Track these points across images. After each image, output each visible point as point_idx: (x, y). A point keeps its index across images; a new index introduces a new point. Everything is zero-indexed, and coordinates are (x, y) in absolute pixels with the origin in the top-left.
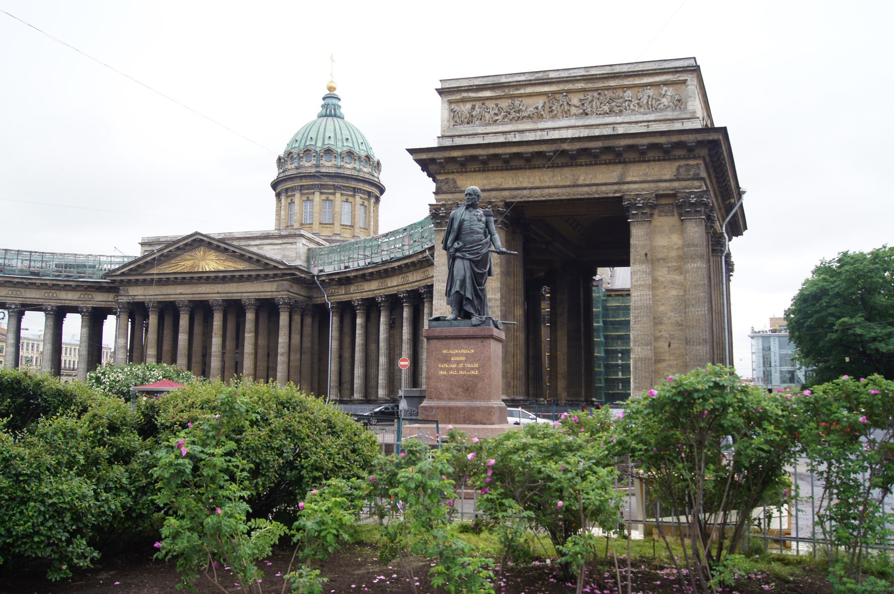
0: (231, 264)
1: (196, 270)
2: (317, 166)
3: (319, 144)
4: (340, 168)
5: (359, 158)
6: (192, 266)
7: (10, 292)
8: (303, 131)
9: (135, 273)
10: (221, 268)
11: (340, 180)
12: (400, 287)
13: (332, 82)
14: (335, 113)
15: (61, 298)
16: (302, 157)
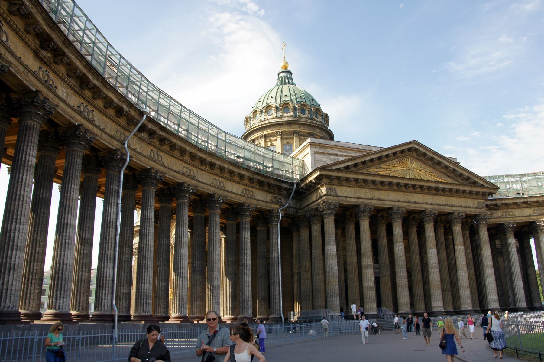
3: (308, 103)
15: (227, 189)
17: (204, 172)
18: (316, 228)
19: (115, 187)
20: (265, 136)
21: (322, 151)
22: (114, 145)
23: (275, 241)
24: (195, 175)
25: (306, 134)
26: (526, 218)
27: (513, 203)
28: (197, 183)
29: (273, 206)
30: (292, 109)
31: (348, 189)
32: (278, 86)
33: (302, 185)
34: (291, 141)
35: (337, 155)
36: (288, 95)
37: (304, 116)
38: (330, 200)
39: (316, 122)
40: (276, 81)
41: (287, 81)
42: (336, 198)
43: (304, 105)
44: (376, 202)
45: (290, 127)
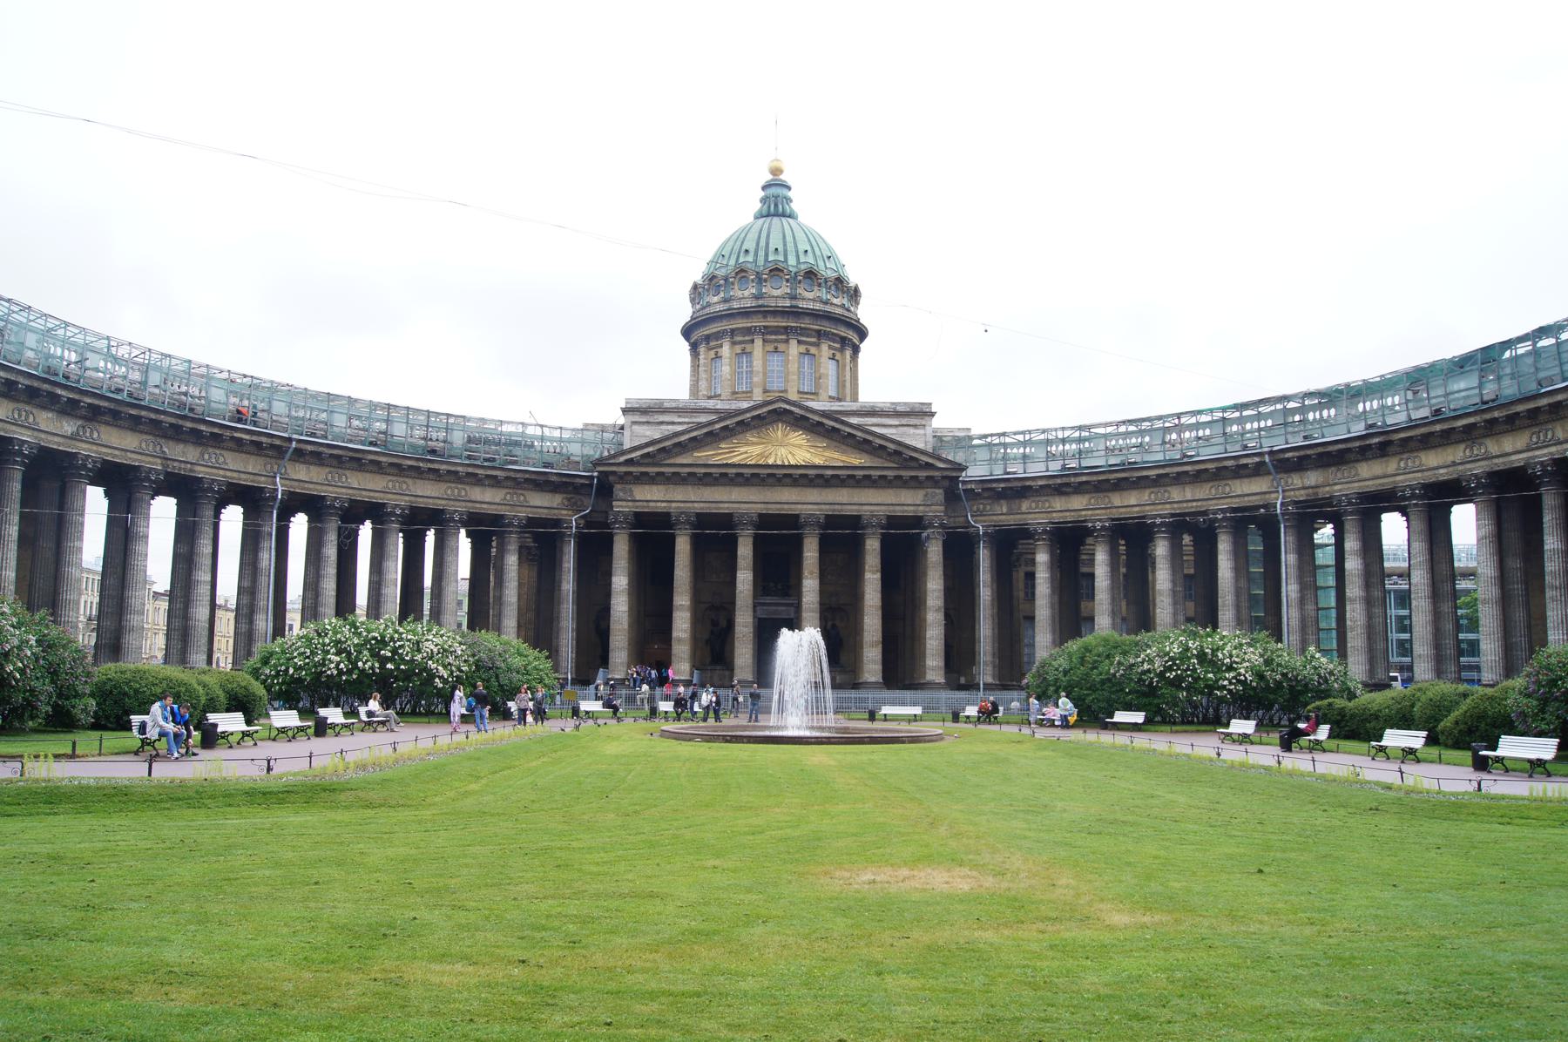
0: (836, 455)
1: (771, 462)
2: (793, 297)
3: (792, 261)
4: (826, 303)
5: (849, 289)
6: (761, 455)
7: (390, 485)
8: (753, 236)
9: (650, 460)
10: (818, 461)
11: (826, 323)
12: (1147, 508)
13: (777, 160)
15: (473, 498)
16: (766, 281)
17: (426, 482)
19: (266, 529)
20: (708, 338)
21: (645, 420)
22: (262, 482)
24: (411, 487)
26: (1073, 514)
27: (1041, 486)
28: (412, 499)
29: (564, 512)
30: (753, 281)
31: (655, 488)
34: (748, 347)
35: (673, 423)
38: (622, 507)
39: (802, 304)
40: (757, 206)
42: (630, 504)
43: (777, 269)
44: (702, 505)
45: (747, 318)
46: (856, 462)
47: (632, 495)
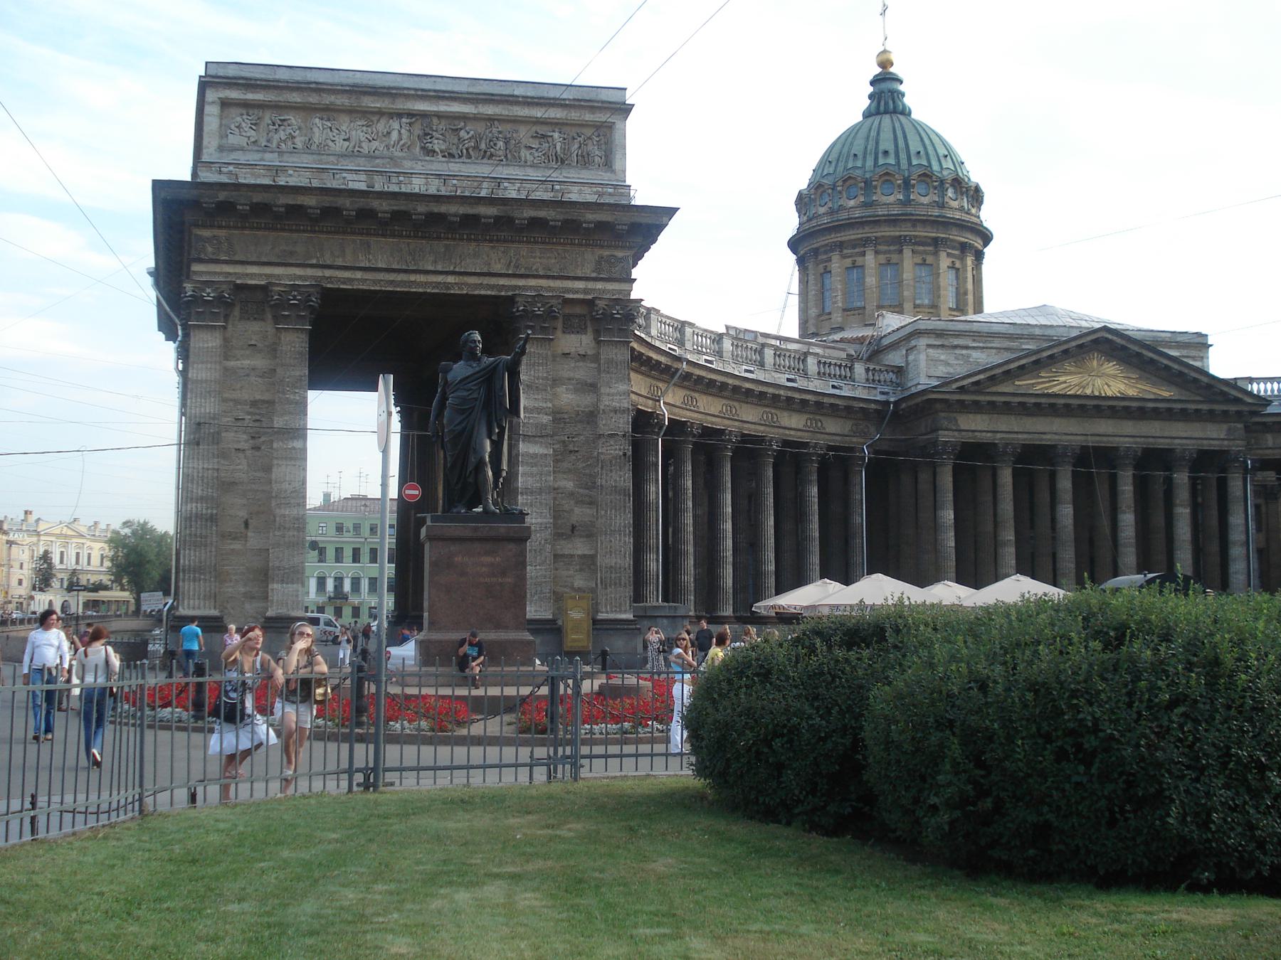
1: (1088, 392)
3: (936, 167)
4: (968, 213)
8: (886, 136)
9: (972, 389)
10: (1131, 392)
14: (895, 107)
15: (783, 424)
16: (913, 186)
18: (924, 476)
19: (653, 459)
20: (841, 246)
23: (858, 497)
25: (929, 241)
29: (854, 440)
30: (899, 186)
31: (979, 417)
32: (871, 119)
33: (904, 405)
34: (895, 258)
35: (967, 348)
36: (891, 148)
37: (925, 200)
41: (891, 103)
42: (956, 433)
43: (925, 175)
44: (1025, 436)
45: (894, 226)
46: (1166, 394)
47: (957, 424)
